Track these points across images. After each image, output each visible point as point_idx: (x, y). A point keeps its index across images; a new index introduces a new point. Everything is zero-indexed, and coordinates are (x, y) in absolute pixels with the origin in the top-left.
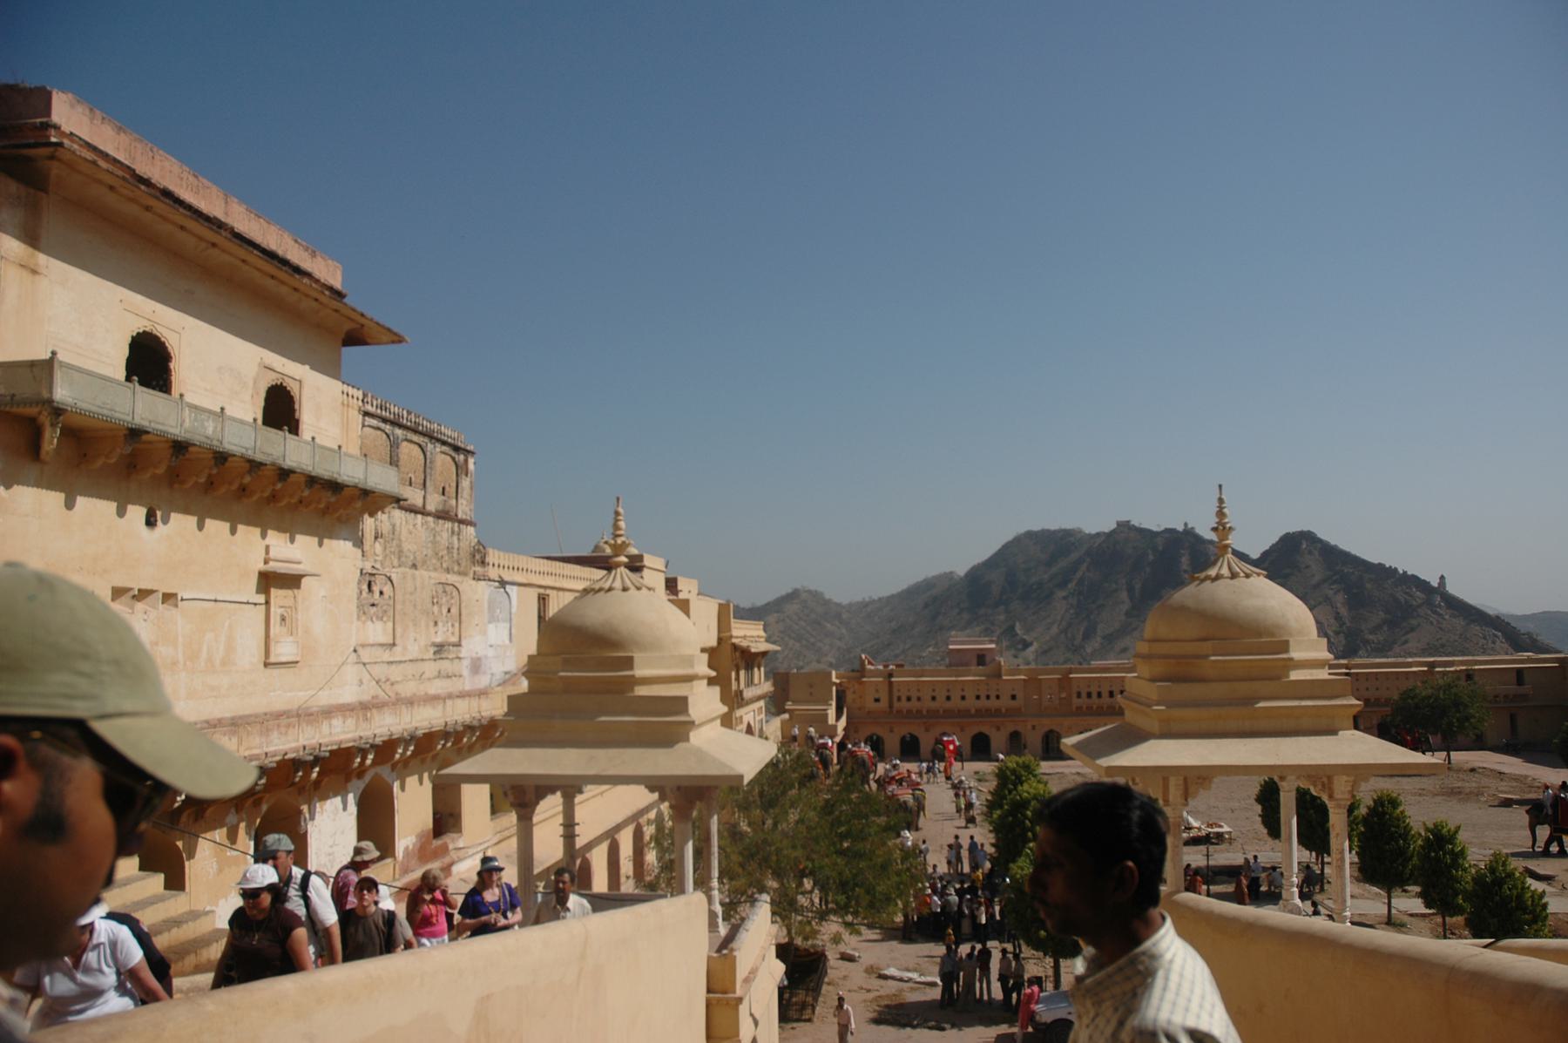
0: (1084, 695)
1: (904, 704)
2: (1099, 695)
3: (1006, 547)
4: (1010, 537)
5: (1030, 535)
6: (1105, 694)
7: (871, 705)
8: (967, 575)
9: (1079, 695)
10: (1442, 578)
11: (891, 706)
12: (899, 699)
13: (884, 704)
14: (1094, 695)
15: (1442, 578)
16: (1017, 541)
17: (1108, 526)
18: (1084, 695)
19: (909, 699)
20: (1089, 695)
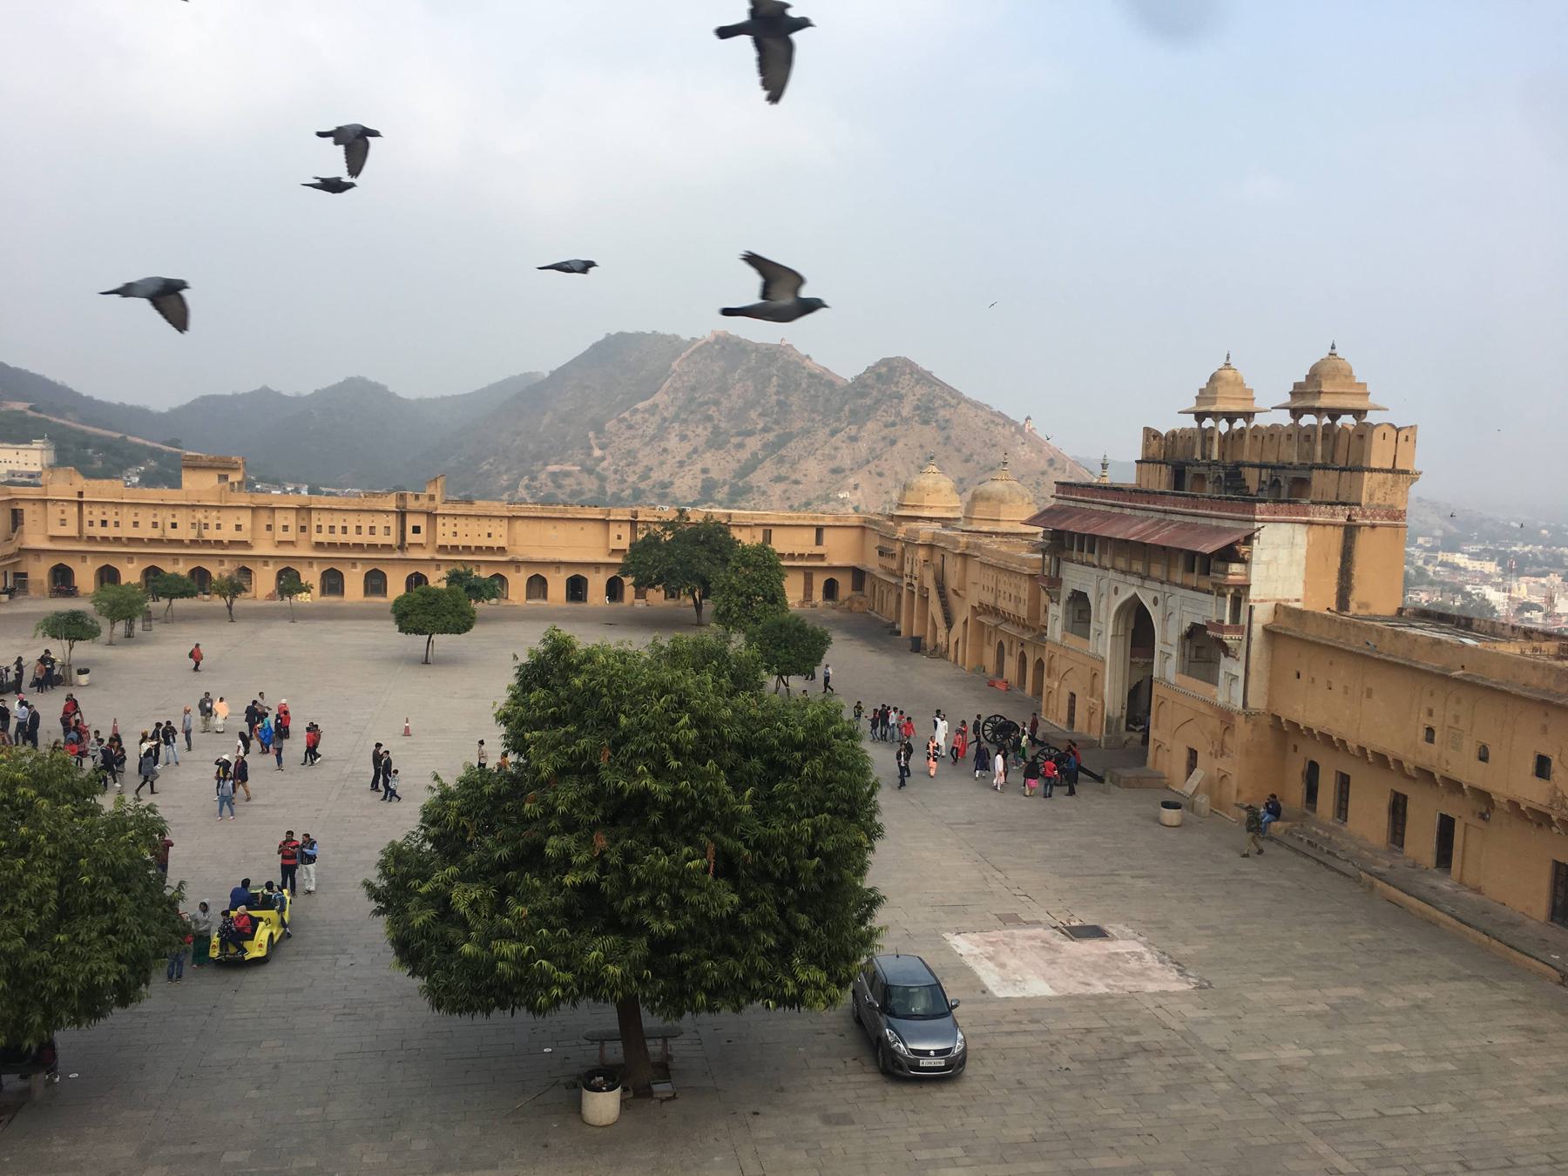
0: (325, 529)
2: (344, 529)
6: (352, 529)
12: (91, 524)
14: (338, 529)
18: (325, 529)
19: (104, 523)
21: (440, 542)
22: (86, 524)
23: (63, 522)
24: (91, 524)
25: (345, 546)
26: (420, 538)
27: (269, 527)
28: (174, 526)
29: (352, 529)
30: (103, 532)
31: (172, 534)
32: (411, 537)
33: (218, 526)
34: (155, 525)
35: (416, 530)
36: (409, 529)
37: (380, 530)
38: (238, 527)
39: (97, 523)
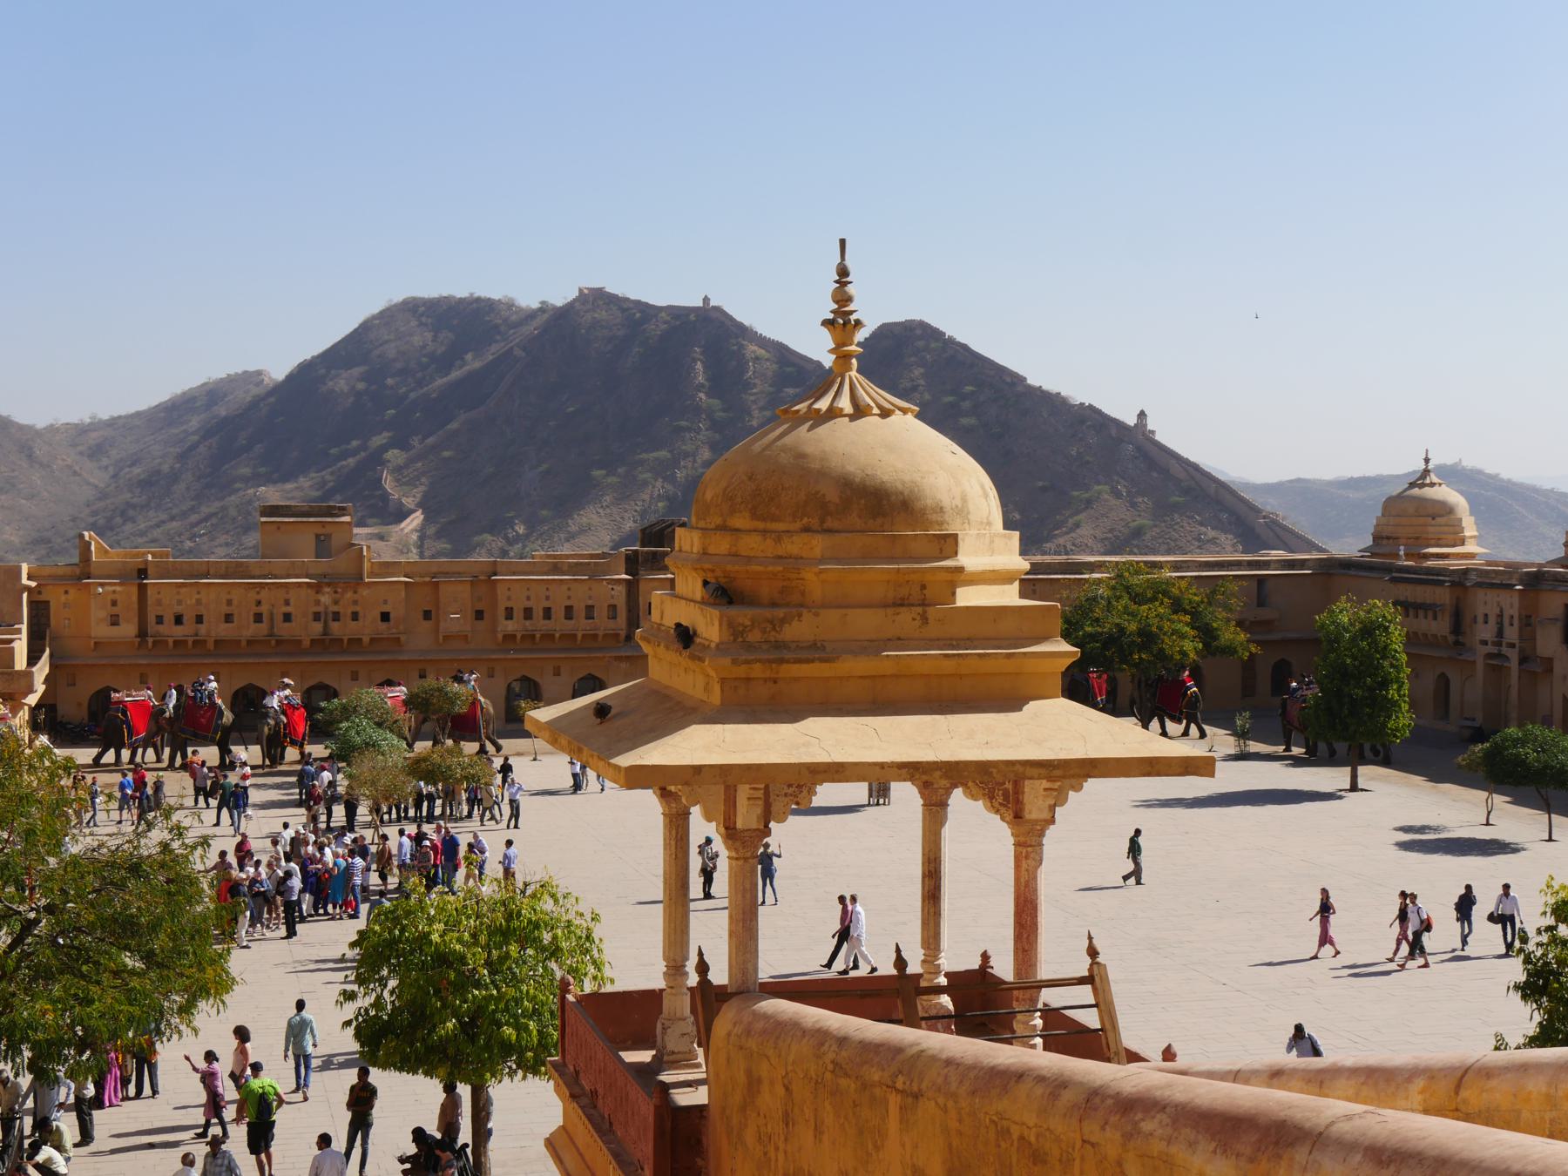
0: (518, 614)
2: (547, 613)
3: (366, 327)
4: (376, 307)
5: (412, 307)
6: (558, 613)
7: (102, 631)
8: (290, 378)
9: (509, 614)
10: (1142, 415)
11: (142, 633)
12: (160, 620)
13: (128, 629)
15: (1142, 415)
16: (388, 316)
17: (561, 295)
18: (518, 614)
19: (179, 620)
20: (528, 613)
22: (151, 619)
23: (115, 621)
24: (160, 620)
27: (427, 615)
29: (558, 613)
30: (179, 632)
31: (284, 630)
33: (355, 617)
34: (258, 618)
37: (601, 613)
38: (385, 617)
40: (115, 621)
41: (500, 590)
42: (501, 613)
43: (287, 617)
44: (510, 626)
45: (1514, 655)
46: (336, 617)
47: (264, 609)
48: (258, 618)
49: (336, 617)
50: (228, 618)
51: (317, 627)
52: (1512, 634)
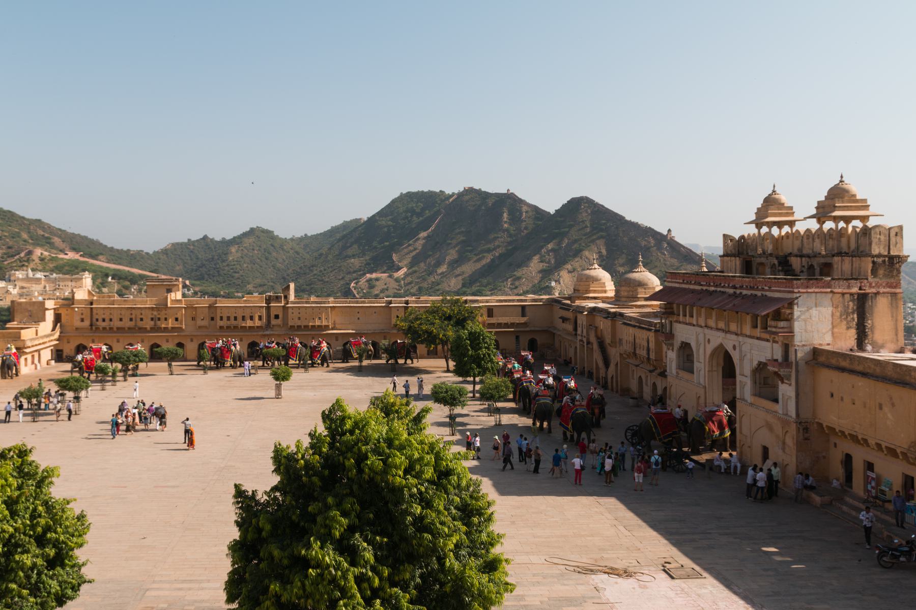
0: (225, 319)
1: (101, 324)
2: (236, 318)
11: (91, 325)
12: (97, 320)
13: (87, 323)
14: (232, 318)
18: (225, 319)
21: (290, 323)
22: (94, 320)
23: (82, 320)
25: (236, 327)
26: (279, 322)
28: (142, 319)
31: (140, 324)
32: (274, 322)
34: (131, 320)
35: (277, 317)
36: (272, 316)
39: (100, 320)
40: (82, 320)
41: (219, 311)
42: (218, 318)
43: (142, 319)
44: (221, 323)
45: (585, 340)
46: (159, 319)
47: (133, 316)
48: (131, 320)
49: (159, 319)
50: (121, 320)
51: (152, 323)
52: (585, 331)
